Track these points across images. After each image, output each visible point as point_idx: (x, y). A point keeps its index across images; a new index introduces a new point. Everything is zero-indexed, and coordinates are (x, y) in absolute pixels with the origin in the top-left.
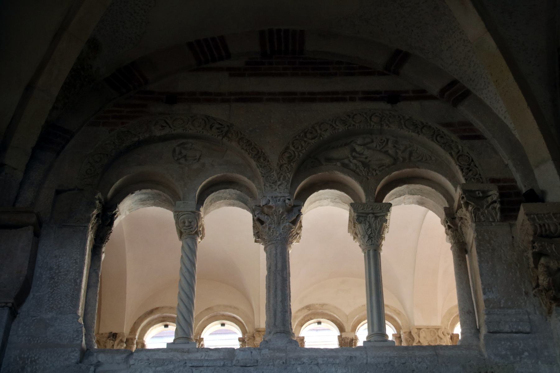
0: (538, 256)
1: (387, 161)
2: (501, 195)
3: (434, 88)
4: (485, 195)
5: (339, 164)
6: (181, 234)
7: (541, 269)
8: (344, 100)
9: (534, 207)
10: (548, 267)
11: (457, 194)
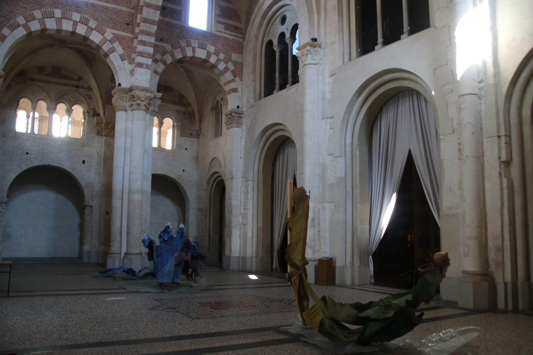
0: (96, 126)
1: (74, 100)
2: (93, 112)
3: (86, 87)
4: (90, 112)
5: (65, 99)
6: (32, 109)
7: (96, 129)
8: (67, 86)
9: (98, 117)
10: (97, 129)
11: (86, 111)
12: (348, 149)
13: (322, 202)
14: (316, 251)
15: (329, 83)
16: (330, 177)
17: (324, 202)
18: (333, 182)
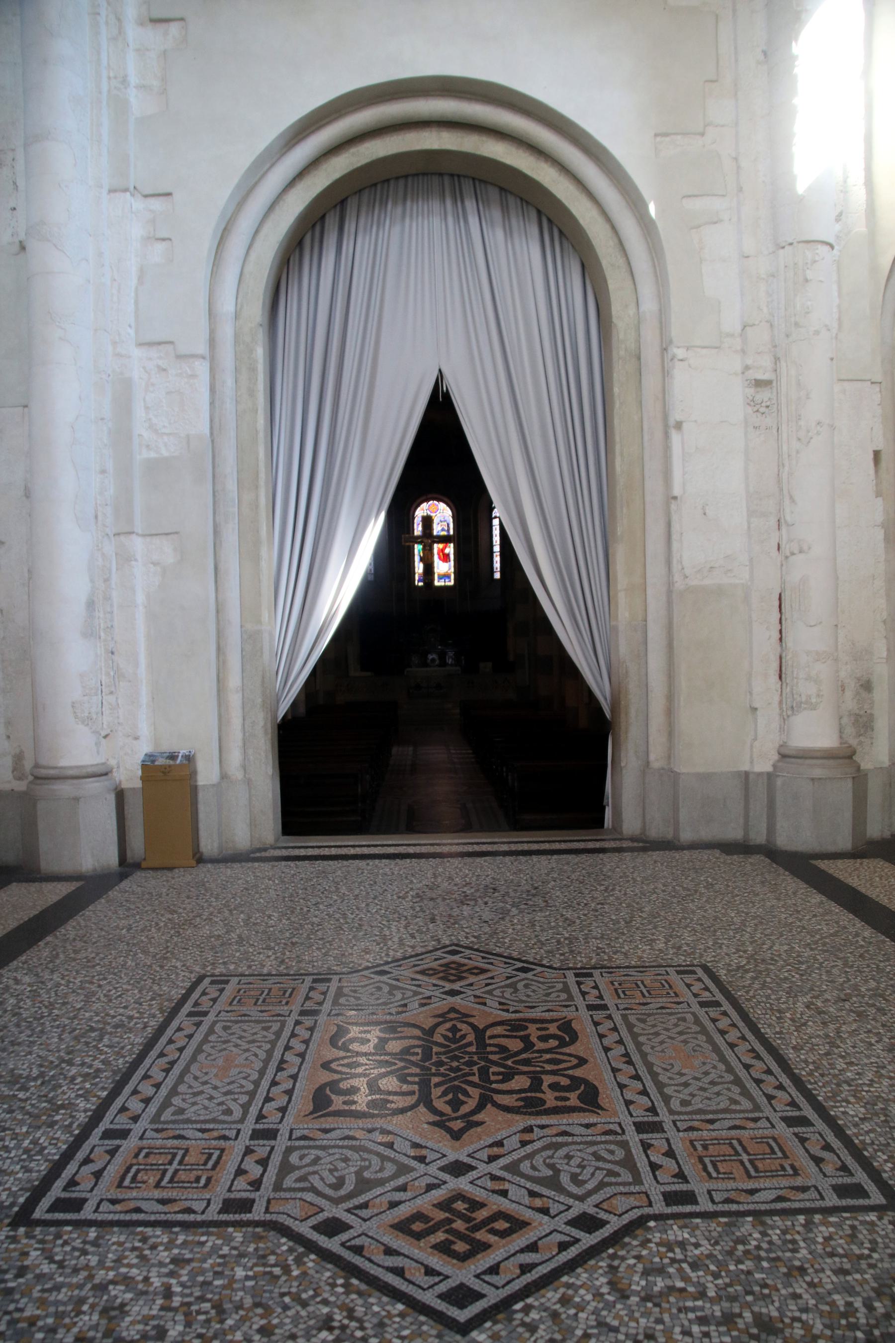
12: (227, 331)
13: (117, 534)
14: (103, 733)
15: (137, 50)
16: (146, 434)
17: (132, 533)
18: (165, 453)
